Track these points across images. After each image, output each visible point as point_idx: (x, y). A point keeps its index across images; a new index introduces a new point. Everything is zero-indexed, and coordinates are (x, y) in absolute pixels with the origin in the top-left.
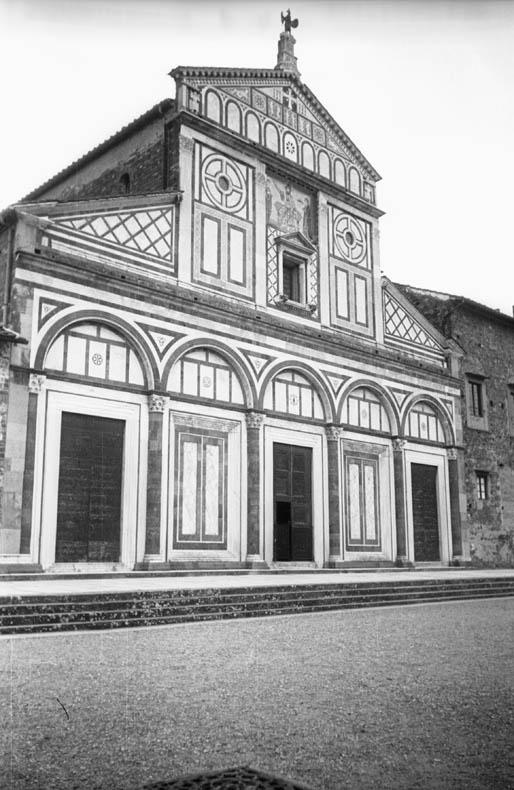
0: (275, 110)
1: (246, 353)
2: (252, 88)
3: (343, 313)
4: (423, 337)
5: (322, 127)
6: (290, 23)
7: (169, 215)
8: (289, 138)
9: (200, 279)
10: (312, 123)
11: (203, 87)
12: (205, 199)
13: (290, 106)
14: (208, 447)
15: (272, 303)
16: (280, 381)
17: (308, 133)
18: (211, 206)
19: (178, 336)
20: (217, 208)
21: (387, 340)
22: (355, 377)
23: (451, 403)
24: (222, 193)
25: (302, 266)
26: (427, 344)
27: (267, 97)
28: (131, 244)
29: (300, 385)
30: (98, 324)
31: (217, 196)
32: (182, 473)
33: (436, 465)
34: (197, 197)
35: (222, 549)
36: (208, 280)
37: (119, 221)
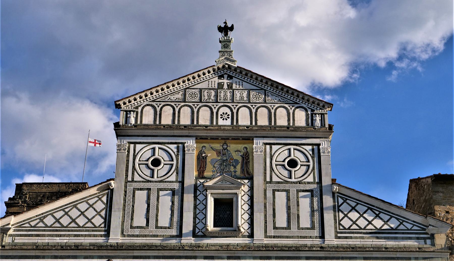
0: (209, 96)
5: (262, 89)
7: (104, 199)
9: (129, 233)
11: (140, 105)
12: (137, 178)
13: (225, 87)
15: (200, 234)
18: (143, 182)
20: (148, 181)
25: (235, 199)
27: (201, 90)
34: (130, 179)
36: (137, 232)
37: (64, 213)
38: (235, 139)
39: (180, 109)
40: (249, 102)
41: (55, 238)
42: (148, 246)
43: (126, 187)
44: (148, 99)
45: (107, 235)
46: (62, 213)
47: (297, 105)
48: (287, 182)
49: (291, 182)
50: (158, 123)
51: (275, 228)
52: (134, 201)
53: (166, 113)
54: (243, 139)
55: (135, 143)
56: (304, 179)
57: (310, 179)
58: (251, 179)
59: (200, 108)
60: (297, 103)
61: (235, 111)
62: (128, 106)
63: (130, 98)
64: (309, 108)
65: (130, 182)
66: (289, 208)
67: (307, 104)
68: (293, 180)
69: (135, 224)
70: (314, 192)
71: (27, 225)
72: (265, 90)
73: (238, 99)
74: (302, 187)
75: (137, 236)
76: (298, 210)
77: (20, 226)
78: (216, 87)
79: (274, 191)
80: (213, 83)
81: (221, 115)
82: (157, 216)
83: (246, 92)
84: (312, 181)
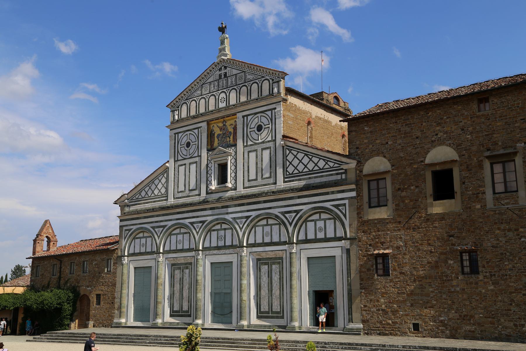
1: (192, 223)
2: (202, 85)
3: (253, 176)
4: (321, 164)
6: (222, 30)
7: (165, 175)
8: (223, 95)
10: (236, 75)
11: (180, 105)
13: (223, 77)
14: (184, 270)
15: (210, 191)
16: (214, 230)
17: (233, 83)
19: (164, 227)
20: (185, 159)
21: (286, 180)
22: (254, 214)
23: (344, 205)
24: (187, 150)
26: (327, 166)
27: (210, 83)
28: (153, 195)
29: (225, 229)
30: (143, 232)
31: (185, 152)
32: (174, 284)
33: (306, 259)
34: (176, 159)
35: (189, 317)
36: (180, 195)
38: (228, 117)
39: (199, 102)
40: (236, 85)
41: (146, 205)
42: (184, 204)
43: (174, 165)
44: (184, 99)
45: (167, 200)
46: (148, 187)
47: (263, 79)
48: (256, 144)
49: (258, 143)
50: (189, 115)
51: (249, 181)
52: (178, 175)
53: (193, 107)
54: (232, 116)
55: (178, 133)
56: (266, 139)
57: (269, 139)
58: (235, 145)
59: (209, 97)
60: (264, 77)
61: (228, 94)
62: (174, 107)
63: (173, 102)
64: (271, 79)
65: (177, 161)
66: (257, 163)
67: (269, 76)
68: (260, 141)
69: (179, 191)
70: (272, 148)
71: (135, 198)
72: (245, 72)
73: (230, 84)
74: (264, 145)
75: (180, 198)
76: (262, 165)
77: (132, 199)
78: (218, 79)
79: (249, 152)
80: (216, 75)
81: (221, 100)
82: (189, 182)
83: (234, 77)
84: (271, 139)
